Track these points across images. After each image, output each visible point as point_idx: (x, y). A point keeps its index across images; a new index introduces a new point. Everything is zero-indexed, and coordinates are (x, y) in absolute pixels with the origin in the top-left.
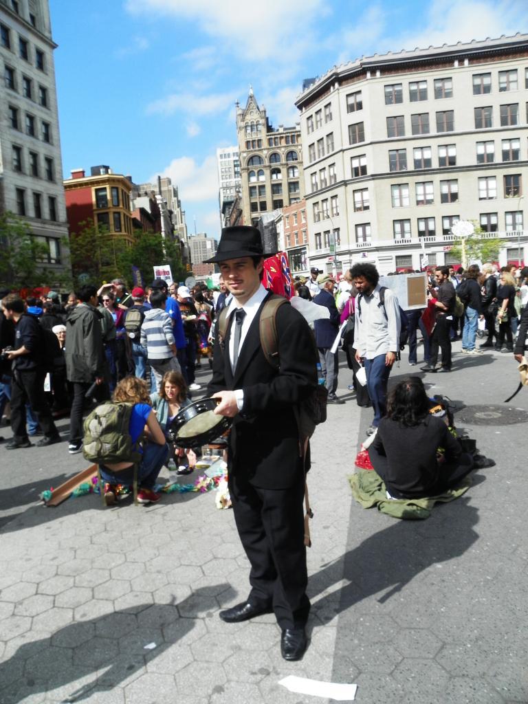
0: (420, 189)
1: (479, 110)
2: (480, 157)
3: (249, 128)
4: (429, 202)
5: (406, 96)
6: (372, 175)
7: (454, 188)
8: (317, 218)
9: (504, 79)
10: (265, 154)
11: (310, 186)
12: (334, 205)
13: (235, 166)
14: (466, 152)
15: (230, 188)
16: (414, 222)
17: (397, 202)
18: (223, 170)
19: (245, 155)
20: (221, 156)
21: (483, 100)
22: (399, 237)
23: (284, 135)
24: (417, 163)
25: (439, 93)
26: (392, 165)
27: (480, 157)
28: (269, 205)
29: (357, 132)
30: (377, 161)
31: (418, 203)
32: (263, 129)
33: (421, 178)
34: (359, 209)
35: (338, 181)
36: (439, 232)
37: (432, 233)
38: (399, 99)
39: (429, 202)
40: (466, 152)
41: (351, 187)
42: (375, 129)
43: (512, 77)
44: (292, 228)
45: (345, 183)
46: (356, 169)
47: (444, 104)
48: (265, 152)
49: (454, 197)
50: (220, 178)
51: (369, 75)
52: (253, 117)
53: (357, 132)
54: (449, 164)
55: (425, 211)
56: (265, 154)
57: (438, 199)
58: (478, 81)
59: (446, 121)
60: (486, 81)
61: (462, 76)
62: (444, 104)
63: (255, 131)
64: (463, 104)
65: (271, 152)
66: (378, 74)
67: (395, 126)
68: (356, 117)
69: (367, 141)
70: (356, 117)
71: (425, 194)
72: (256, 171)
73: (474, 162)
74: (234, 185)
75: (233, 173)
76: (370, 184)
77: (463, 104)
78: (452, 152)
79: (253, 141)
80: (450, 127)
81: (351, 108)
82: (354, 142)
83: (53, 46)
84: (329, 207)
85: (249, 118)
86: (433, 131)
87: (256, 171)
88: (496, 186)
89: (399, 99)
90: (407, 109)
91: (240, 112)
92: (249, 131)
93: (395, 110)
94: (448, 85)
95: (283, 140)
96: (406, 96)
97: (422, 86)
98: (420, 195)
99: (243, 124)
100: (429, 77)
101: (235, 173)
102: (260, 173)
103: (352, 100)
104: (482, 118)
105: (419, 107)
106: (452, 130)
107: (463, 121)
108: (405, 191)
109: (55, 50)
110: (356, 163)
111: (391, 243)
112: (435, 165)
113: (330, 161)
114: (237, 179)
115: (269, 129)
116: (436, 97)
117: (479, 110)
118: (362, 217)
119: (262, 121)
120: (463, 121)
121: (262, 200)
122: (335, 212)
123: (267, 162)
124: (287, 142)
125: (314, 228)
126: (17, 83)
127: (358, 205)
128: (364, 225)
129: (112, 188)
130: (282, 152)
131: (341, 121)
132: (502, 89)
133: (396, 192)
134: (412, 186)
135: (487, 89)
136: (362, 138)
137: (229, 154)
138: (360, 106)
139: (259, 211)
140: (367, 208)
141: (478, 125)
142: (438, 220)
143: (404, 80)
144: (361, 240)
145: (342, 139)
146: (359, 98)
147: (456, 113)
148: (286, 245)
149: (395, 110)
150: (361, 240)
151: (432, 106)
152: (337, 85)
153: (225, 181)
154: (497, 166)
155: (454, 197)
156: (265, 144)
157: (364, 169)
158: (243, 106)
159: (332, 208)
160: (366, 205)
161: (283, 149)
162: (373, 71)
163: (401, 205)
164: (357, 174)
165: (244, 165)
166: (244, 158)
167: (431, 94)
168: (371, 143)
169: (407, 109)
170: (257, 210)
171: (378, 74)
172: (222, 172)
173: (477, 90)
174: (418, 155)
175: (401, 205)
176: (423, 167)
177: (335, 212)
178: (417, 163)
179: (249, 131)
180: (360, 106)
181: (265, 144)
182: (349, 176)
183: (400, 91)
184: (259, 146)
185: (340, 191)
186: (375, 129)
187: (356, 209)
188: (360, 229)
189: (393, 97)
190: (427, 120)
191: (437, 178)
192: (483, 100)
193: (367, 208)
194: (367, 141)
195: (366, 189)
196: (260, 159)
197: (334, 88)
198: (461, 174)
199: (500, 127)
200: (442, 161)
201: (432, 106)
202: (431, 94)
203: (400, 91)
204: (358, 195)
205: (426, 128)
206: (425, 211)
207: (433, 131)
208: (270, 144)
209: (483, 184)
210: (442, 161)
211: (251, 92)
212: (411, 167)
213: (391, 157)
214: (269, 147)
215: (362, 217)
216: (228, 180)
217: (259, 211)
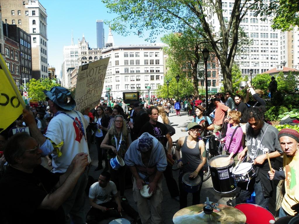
0: (132, 77)
1: (145, 60)
3: (82, 48)
4: (134, 80)
5: (129, 55)
9: (151, 54)
10: (88, 57)
13: (71, 53)
14: (142, 69)
15: (69, 61)
16: (130, 85)
17: (126, 80)
18: (66, 54)
19: (81, 56)
20: (66, 49)
21: (146, 58)
22: (126, 88)
24: (131, 71)
25: (136, 56)
26: (125, 71)
27: (145, 71)
30: (122, 70)
32: (87, 49)
33: (132, 75)
34: (117, 81)
35: (112, 74)
36: (136, 88)
37: (134, 88)
38: (127, 56)
39: (134, 80)
40: (142, 69)
42: (122, 63)
43: (153, 54)
46: (117, 71)
47: (137, 58)
49: (139, 80)
50: (65, 57)
51: (120, 50)
52: (84, 44)
53: (117, 63)
54: (138, 72)
55: (133, 83)
56: (88, 57)
57: (136, 80)
58: (145, 54)
59: (138, 62)
60: (147, 54)
61: (142, 52)
62: (137, 58)
63: (84, 49)
64: (142, 59)
65: (90, 56)
66: (123, 50)
67: (126, 62)
68: (117, 59)
69: (120, 65)
70: (117, 59)
72: (84, 62)
73: (144, 72)
77: (142, 59)
78: (139, 69)
79: (84, 52)
80: (139, 63)
81: (116, 57)
82: (116, 65)
83: (47, 40)
84: (110, 80)
85: (83, 45)
86: (135, 64)
87: (84, 62)
88: (149, 78)
89: (127, 56)
90: (129, 59)
91: (80, 42)
92: (82, 49)
93: (126, 58)
94: (139, 54)
95: (94, 53)
96: (129, 55)
97: (133, 54)
99: (81, 46)
100: (134, 52)
101: (71, 56)
103: (116, 55)
104: (146, 62)
105: (132, 58)
106: (139, 64)
107: (142, 63)
108: (128, 78)
109: (48, 41)
110: (117, 70)
112: (135, 72)
113: (111, 68)
114: (72, 58)
115: (89, 49)
117: (145, 60)
118: (118, 83)
119: (87, 46)
120: (142, 63)
123: (88, 59)
124: (95, 53)
126: (40, 50)
127: (117, 80)
128: (118, 85)
129: (52, 71)
130: (93, 56)
132: (150, 56)
133: (126, 78)
134: (130, 77)
135: (147, 56)
136: (118, 64)
137: (69, 49)
138: (118, 57)
140: (119, 81)
141: (145, 64)
142: (136, 85)
143: (129, 52)
144: (117, 88)
146: (118, 55)
147: (140, 61)
150: (117, 88)
151: (135, 58)
152: (113, 50)
153: (67, 58)
154: (149, 73)
155: (139, 80)
156: (87, 53)
157: (118, 72)
158: (81, 40)
161: (93, 56)
162: (122, 49)
163: (127, 81)
164: (117, 73)
165: (80, 59)
166: (81, 57)
167: (135, 56)
169: (129, 59)
171: (123, 50)
172: (66, 55)
173: (145, 56)
174: (131, 70)
175: (127, 81)
176: (132, 72)
178: (131, 71)
179: (82, 49)
180: (118, 57)
181: (87, 53)
182: (115, 73)
183: (128, 54)
184: (86, 54)
186: (122, 63)
187: (116, 81)
188: (117, 86)
189: (126, 55)
190: (134, 62)
191: (136, 75)
192: (146, 58)
193: (119, 81)
195: (119, 77)
196: (86, 58)
200: (137, 71)
201: (135, 58)
202: (135, 56)
203: (128, 54)
204: (117, 78)
206: (133, 83)
207: (135, 64)
208: (89, 54)
209: (146, 77)
210: (137, 71)
211: (84, 36)
212: (129, 72)
213: (125, 69)
214: (88, 54)
215: (118, 83)
216: (68, 58)
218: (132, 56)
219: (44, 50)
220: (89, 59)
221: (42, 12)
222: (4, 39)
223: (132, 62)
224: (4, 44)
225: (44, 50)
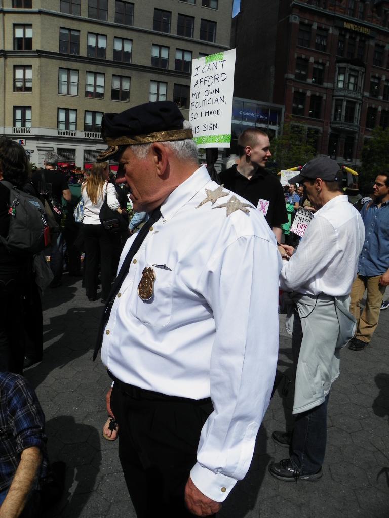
2: (156, 60)
6: (38, 51)
7: (126, 86)
17: (64, 89)
31: (88, 94)
34: (20, 89)
41: (11, 61)
57: (109, 95)
71: (95, 86)
76: (35, 62)
98: (90, 85)
110: (19, 33)
111: (53, 132)
112: (109, 56)
127: (19, 85)
128: (24, 109)
140: (29, 89)
144: (19, 125)
150: (19, 125)
154: (168, 73)
157: (29, 41)
160: (28, 85)
163: (68, 92)
164: (20, 47)
168: (40, 12)
175: (68, 92)
176: (96, 57)
187: (16, 89)
191: (111, 71)
194: (35, 8)
198: (134, 73)
199: (176, 35)
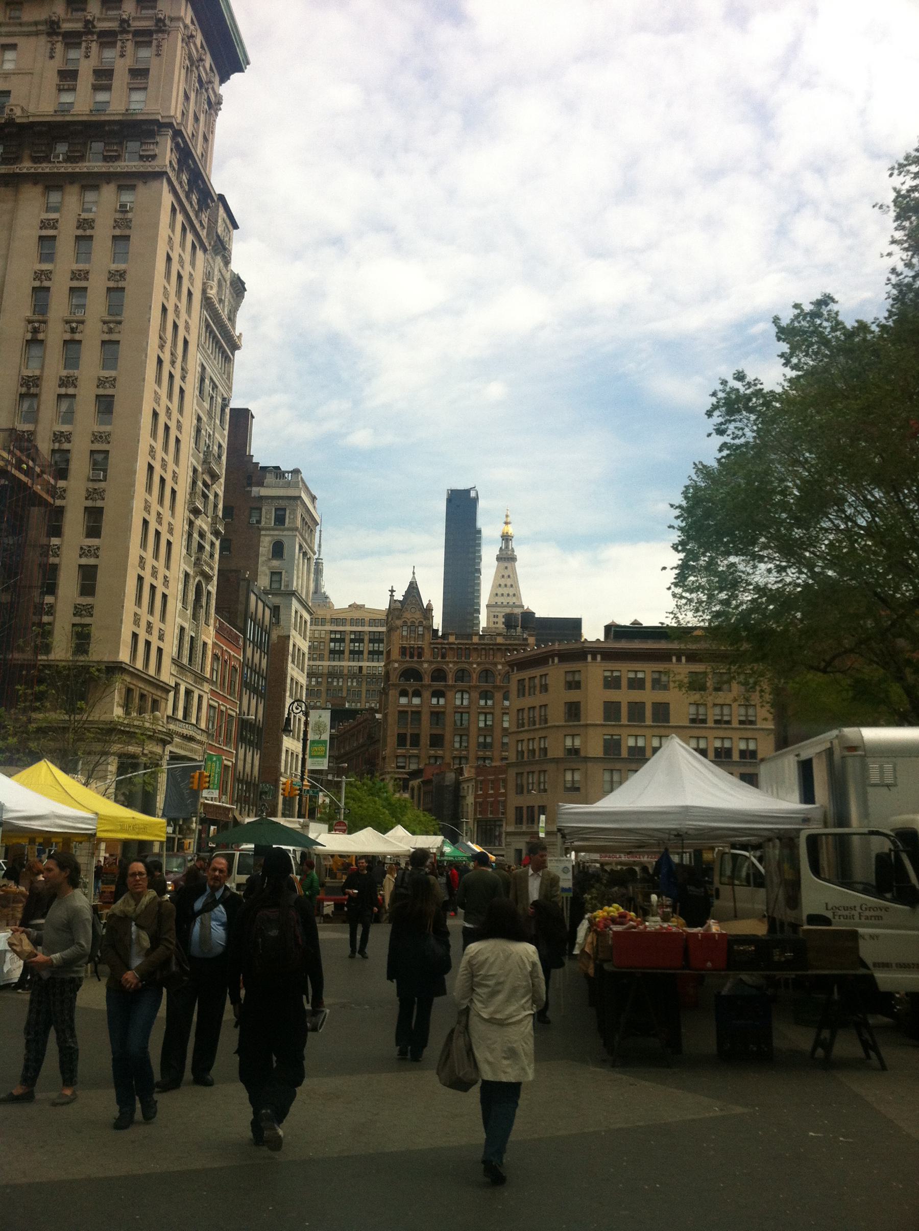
5: (624, 683)
8: (520, 790)
11: (515, 753)
12: (542, 780)
23: (455, 646)
28: (425, 740)
29: (574, 711)
44: (486, 795)
45: (556, 761)
48: (426, 665)
67: (611, 710)
70: (573, 696)
74: (326, 671)
75: (326, 653)
90: (624, 696)
93: (613, 695)
96: (624, 683)
100: (646, 671)
102: (417, 694)
105: (636, 696)
116: (653, 688)
121: (416, 732)
122: (542, 787)
123: (427, 680)
125: (514, 801)
127: (569, 785)
130: (451, 668)
131: (557, 698)
139: (408, 747)
143: (626, 670)
145: (557, 715)
148: (475, 814)
149: (613, 695)
151: (648, 696)
159: (539, 783)
160: (577, 785)
167: (648, 685)
169: (624, 696)
170: (405, 745)
177: (542, 787)
185: (551, 767)
189: (612, 683)
193: (578, 789)
197: (553, 662)
205: (642, 718)
212: (624, 754)
217: (408, 747)
218: (637, 684)
219: (299, 650)
220: (434, 679)
221: (308, 511)
222: (215, 627)
223: (636, 711)
224: (214, 644)
225: (299, 650)
